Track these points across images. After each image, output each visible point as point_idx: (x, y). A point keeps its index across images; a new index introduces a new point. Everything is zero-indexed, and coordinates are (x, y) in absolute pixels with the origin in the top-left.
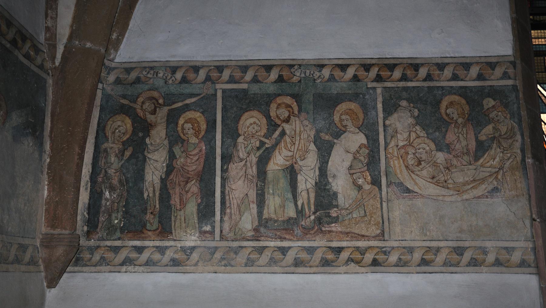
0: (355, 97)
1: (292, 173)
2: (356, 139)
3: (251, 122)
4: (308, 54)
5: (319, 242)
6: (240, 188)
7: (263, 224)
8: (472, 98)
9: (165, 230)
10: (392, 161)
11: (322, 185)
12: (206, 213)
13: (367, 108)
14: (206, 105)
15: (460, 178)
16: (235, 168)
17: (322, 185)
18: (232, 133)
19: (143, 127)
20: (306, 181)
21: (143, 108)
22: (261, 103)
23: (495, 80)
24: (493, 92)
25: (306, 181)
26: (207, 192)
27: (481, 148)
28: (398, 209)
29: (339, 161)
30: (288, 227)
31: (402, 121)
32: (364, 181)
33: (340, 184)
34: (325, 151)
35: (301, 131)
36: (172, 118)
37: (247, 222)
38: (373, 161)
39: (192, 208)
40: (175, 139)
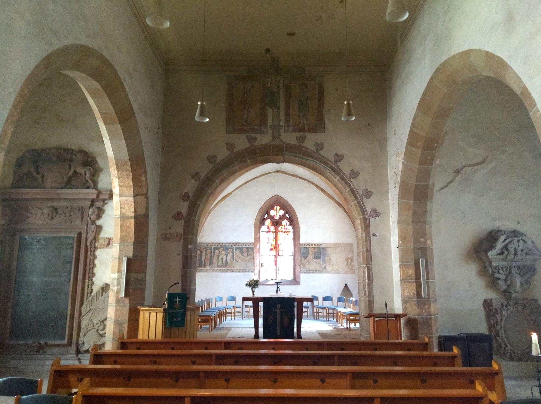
0: (231, 248)
1: (222, 259)
2: (231, 254)
3: (217, 251)
4: (225, 242)
5: (226, 268)
6: (215, 261)
7: (218, 266)
8: (247, 248)
9: (205, 267)
10: (235, 257)
11: (226, 261)
12: (210, 264)
13: (233, 250)
14: (211, 249)
15: (245, 260)
16: (214, 258)
17: (226, 261)
18: (214, 253)
19: (202, 252)
20: (224, 260)
21: (202, 249)
22: (218, 249)
23: (251, 246)
24: (250, 248)
25: (224, 260)
26: (211, 262)
27: (248, 256)
28: (236, 264)
29: (229, 257)
30: (221, 266)
31: (238, 252)
32: (232, 260)
33: (229, 261)
34: (227, 256)
35: (223, 253)
36: (206, 251)
37: (216, 266)
38: (233, 258)
39: (208, 264)
40: (206, 254)
